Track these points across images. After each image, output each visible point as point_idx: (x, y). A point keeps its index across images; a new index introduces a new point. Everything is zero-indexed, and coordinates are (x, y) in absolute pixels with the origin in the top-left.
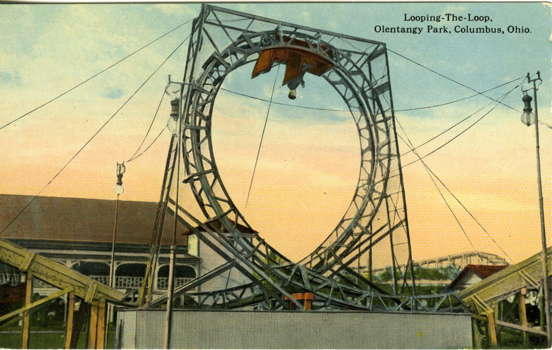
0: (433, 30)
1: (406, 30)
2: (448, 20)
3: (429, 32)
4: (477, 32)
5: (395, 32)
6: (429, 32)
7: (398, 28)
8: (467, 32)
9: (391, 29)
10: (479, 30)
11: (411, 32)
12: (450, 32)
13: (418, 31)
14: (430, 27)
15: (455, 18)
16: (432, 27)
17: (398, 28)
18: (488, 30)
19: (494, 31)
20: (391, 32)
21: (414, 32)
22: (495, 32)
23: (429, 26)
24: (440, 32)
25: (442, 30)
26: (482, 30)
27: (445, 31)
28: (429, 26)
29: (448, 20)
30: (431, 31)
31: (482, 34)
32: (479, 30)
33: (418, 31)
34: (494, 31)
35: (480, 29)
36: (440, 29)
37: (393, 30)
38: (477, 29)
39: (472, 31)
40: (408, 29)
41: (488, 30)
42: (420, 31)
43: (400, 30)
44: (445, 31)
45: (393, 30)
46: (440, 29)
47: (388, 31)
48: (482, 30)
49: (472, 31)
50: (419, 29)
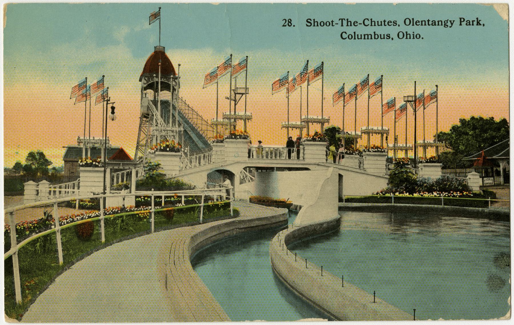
0: (465, 22)
1: (437, 23)
2: (342, 25)
3: (461, 25)
4: (365, 39)
5: (425, 25)
6: (461, 25)
7: (428, 21)
8: (355, 39)
9: (422, 21)
10: (366, 36)
11: (442, 25)
12: (484, 25)
13: (449, 24)
14: (462, 20)
15: (349, 23)
16: (464, 20)
17: (428, 21)
18: (376, 37)
19: (382, 37)
20: (422, 25)
21: (446, 26)
22: (384, 38)
23: (461, 19)
24: (473, 25)
25: (475, 23)
26: (370, 36)
27: (478, 23)
28: (461, 19)
29: (342, 25)
30: (464, 23)
31: (370, 40)
32: (366, 36)
33: (449, 24)
34: (382, 37)
35: (368, 35)
36: (473, 21)
37: (423, 23)
38: (365, 35)
39: (360, 37)
40: (438, 22)
41: (376, 37)
42: (452, 24)
43: (430, 23)
44: (478, 23)
45: (423, 23)
46: (473, 21)
47: (418, 24)
48: (370, 36)
49: (360, 37)
50: (450, 21)
